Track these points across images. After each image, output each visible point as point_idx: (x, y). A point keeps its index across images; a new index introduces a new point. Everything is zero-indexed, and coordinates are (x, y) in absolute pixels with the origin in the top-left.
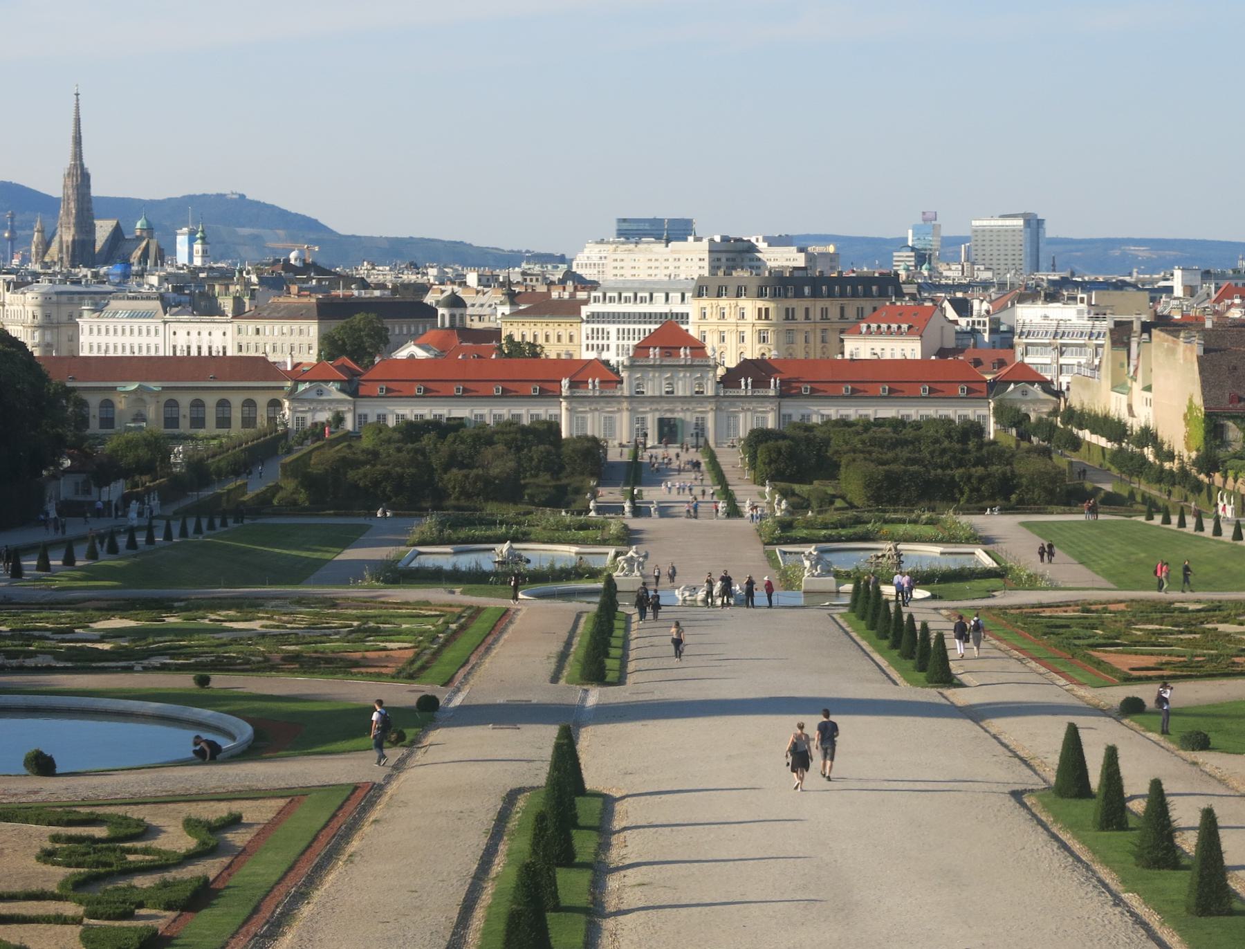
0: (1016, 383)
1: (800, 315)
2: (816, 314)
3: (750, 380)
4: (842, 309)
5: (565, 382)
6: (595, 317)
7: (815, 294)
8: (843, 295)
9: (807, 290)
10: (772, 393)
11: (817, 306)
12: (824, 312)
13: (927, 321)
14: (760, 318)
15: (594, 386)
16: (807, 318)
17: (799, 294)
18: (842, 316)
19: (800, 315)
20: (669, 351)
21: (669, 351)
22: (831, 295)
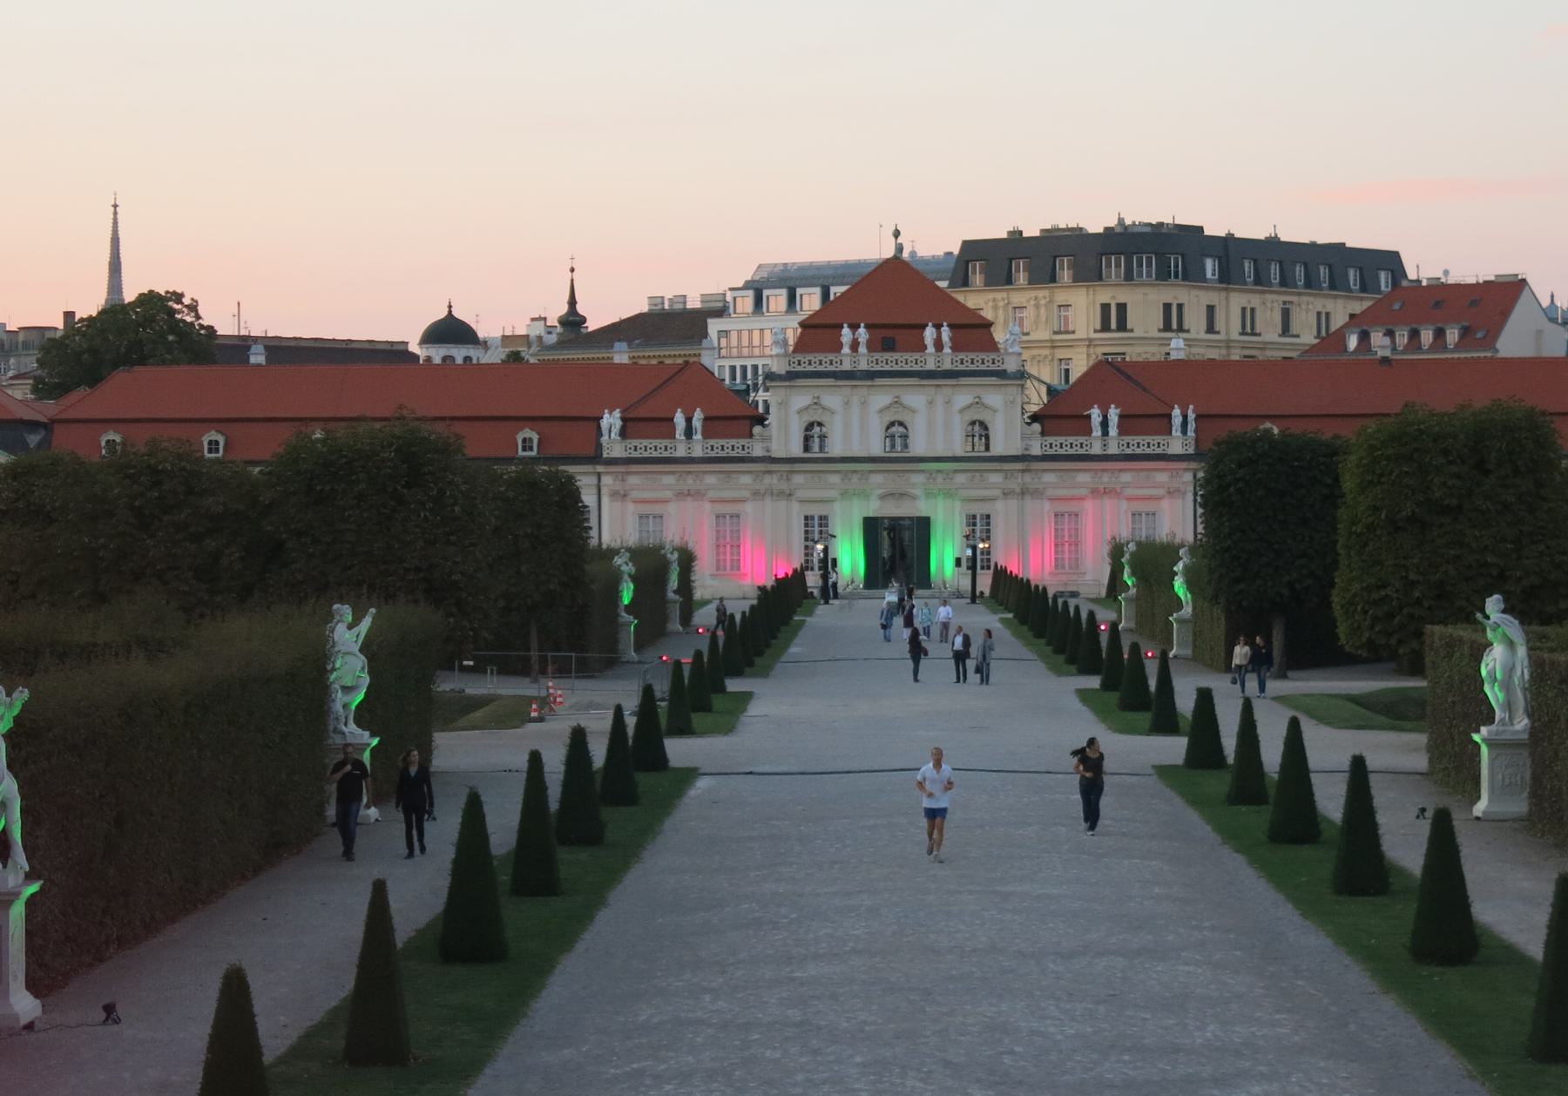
1: (1195, 321)
3: (1114, 414)
4: (1286, 314)
5: (611, 421)
7: (1228, 277)
10: (1177, 443)
12: (1248, 315)
13: (1505, 314)
14: (1105, 327)
15: (689, 432)
16: (1211, 329)
17: (1192, 275)
18: (1286, 330)
19: (1195, 321)
20: (893, 335)
21: (893, 335)
22: (1260, 280)
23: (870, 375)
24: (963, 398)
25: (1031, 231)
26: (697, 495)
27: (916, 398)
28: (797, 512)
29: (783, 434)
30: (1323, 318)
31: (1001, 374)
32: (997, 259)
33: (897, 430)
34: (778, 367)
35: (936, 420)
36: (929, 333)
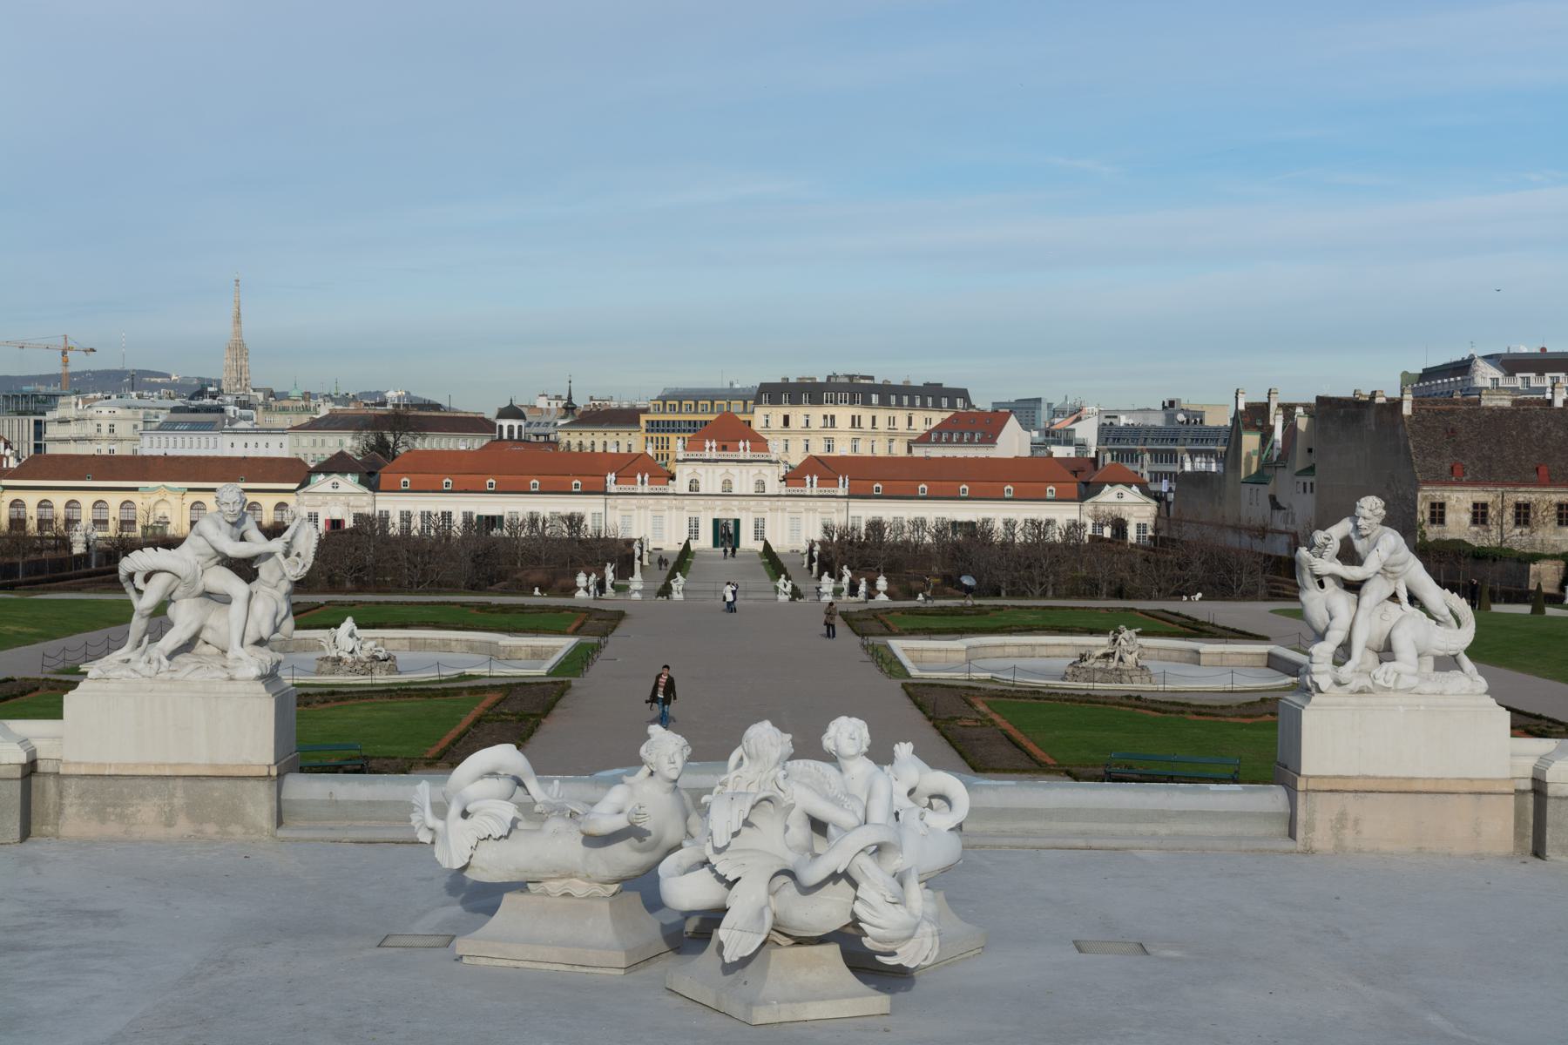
0: (1112, 484)
1: (866, 423)
2: (882, 424)
5: (611, 477)
6: (654, 426)
7: (885, 403)
8: (912, 405)
9: (875, 398)
10: (841, 491)
11: (882, 415)
17: (867, 403)
19: (866, 423)
22: (900, 404)
23: (717, 461)
24: (753, 469)
25: (793, 380)
26: (646, 508)
27: (734, 469)
28: (685, 516)
29: (681, 485)
30: (928, 421)
31: (770, 461)
32: (772, 393)
33: (727, 483)
34: (680, 457)
35: (744, 478)
36: (741, 444)
